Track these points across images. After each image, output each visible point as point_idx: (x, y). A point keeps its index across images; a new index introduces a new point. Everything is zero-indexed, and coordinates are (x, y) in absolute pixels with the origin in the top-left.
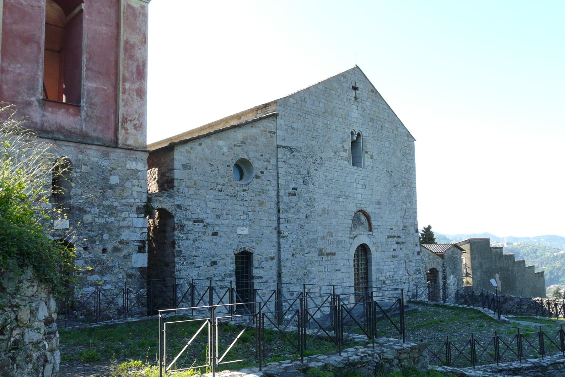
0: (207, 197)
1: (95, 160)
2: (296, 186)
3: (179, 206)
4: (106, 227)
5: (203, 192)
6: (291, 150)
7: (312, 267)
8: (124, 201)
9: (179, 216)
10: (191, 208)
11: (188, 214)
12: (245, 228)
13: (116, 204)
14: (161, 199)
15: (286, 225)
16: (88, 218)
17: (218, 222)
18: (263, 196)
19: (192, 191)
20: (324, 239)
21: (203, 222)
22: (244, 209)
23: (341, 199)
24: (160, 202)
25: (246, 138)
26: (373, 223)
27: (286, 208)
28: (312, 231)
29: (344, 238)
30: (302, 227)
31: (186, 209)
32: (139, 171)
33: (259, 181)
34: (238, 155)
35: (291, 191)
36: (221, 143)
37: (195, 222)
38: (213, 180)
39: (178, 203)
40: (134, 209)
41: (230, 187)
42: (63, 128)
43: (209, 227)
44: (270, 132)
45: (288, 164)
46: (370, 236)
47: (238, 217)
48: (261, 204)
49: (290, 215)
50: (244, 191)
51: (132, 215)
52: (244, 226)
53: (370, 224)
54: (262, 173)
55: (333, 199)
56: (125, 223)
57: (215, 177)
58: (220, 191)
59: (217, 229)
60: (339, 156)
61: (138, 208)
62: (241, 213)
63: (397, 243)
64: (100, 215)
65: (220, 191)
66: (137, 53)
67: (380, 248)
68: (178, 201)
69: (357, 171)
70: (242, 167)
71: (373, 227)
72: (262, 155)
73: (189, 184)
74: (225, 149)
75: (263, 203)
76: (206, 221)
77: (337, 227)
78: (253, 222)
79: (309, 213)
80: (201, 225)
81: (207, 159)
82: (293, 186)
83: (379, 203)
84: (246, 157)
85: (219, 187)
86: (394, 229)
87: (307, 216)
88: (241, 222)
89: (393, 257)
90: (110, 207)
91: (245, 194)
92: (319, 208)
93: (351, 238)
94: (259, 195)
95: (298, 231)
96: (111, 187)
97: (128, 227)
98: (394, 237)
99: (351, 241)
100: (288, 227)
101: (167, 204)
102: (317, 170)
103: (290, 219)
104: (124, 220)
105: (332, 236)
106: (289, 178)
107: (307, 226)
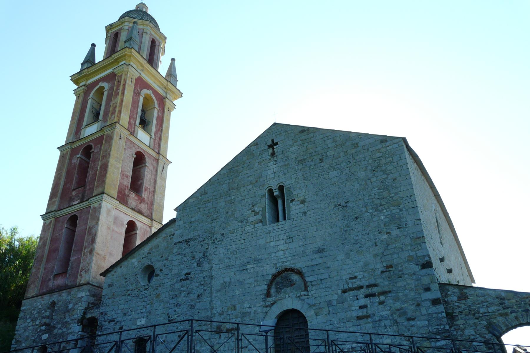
0: (119, 302)
1: (64, 298)
2: (189, 271)
3: (102, 313)
4: (62, 335)
5: (117, 299)
6: (187, 241)
7: (201, 346)
8: (72, 317)
9: (101, 319)
10: (109, 313)
11: (106, 317)
12: (143, 319)
13: (69, 320)
14: (92, 311)
15: (174, 309)
16: (55, 331)
17: (125, 318)
18: (160, 289)
19: (111, 300)
20: (223, 314)
21: (114, 321)
22: (144, 304)
23: (249, 266)
24: (92, 313)
25: (151, 249)
26: (307, 279)
27: (177, 293)
28: (205, 309)
29: (254, 309)
30: (192, 307)
31: (106, 314)
32: (82, 297)
33: (158, 278)
34: (143, 264)
35: (183, 277)
36: (134, 260)
37: (109, 322)
38: (124, 289)
39: (101, 311)
40: (76, 321)
41: (136, 290)
42: (59, 285)
43: (118, 324)
44: (170, 236)
45: (183, 254)
46: (303, 297)
47: (139, 311)
48: (158, 296)
49: (179, 299)
50: (145, 289)
51: (74, 325)
52: (142, 317)
53: (305, 282)
54: (161, 270)
55: (238, 269)
56: (69, 331)
57: (127, 286)
58: (129, 295)
59: (123, 324)
60: (248, 222)
61: (79, 320)
62: (141, 308)
63: (367, 296)
64: (61, 329)
65: (129, 295)
66: (93, 231)
67: (325, 311)
68: (101, 310)
69: (275, 228)
70: (150, 272)
71: (309, 284)
72: (162, 257)
73: (109, 297)
74: (136, 264)
75: (159, 294)
76: (116, 320)
77: (243, 297)
78: (150, 313)
79: (201, 291)
80: (113, 323)
81: (123, 275)
82: (186, 272)
83: (320, 251)
84: (150, 263)
85: (129, 292)
86: (359, 277)
87: (199, 296)
88: (140, 315)
89: (359, 318)
90: (66, 322)
91: (146, 291)
92: (217, 283)
93: (266, 306)
94: (157, 289)
95: (187, 312)
96: (68, 311)
97: (71, 333)
98: (362, 287)
99: (265, 309)
100: (177, 310)
101: (94, 313)
102: (216, 248)
103: (180, 303)
104: (70, 329)
105: (235, 310)
106: (182, 266)
107: (198, 306)
